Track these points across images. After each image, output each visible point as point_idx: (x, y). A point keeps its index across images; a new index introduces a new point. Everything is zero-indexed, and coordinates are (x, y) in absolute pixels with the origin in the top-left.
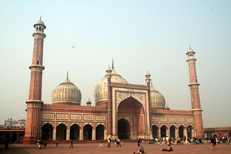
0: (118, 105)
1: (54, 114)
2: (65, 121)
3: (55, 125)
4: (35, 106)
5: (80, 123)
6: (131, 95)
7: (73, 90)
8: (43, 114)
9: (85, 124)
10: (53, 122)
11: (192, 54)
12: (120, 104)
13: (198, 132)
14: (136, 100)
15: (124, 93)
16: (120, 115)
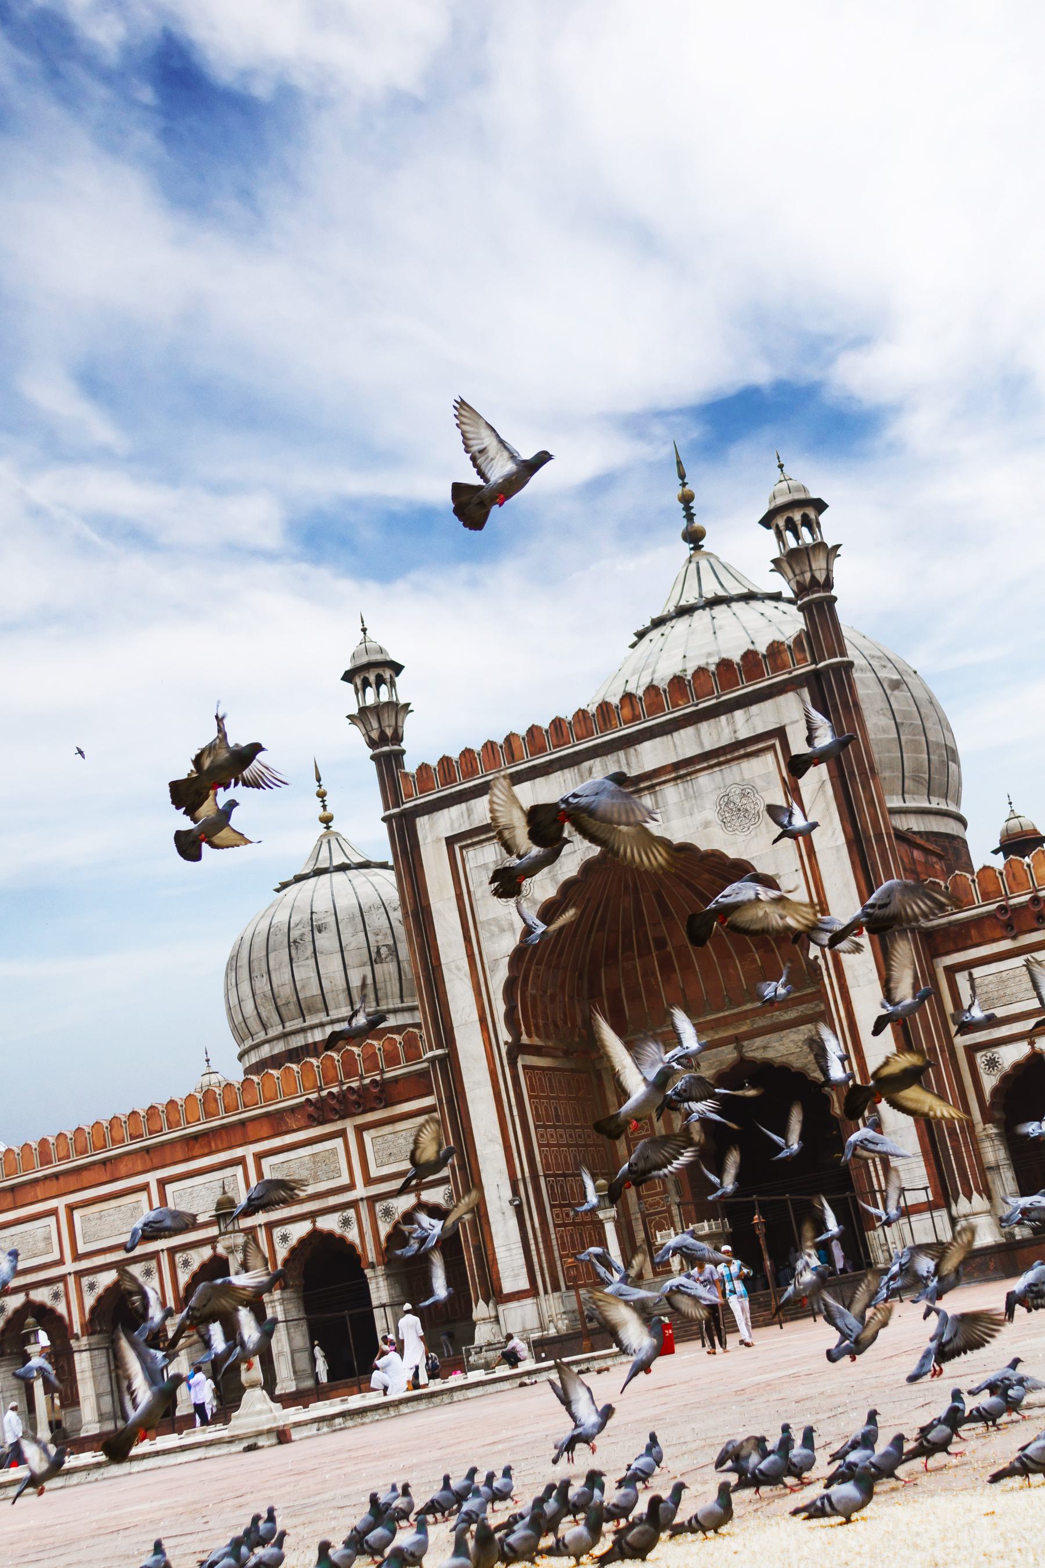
0: (498, 978)
1: (53, 1219)
7: (295, 934)
9: (285, 1238)
10: (61, 1285)
12: (518, 957)
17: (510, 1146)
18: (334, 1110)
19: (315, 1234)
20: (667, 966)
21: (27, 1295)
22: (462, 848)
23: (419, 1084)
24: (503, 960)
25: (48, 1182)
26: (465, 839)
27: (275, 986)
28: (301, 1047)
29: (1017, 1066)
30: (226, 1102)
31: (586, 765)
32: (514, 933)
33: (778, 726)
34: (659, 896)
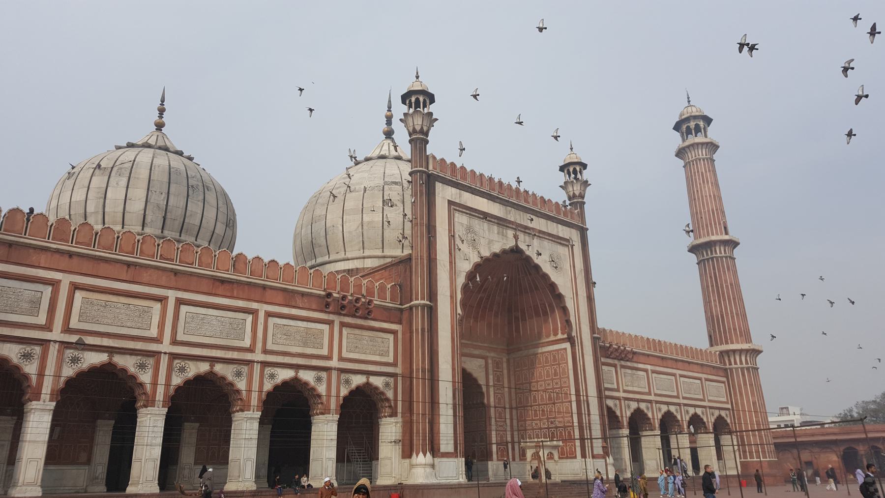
0: (461, 280)
1: (50, 289)
2: (139, 345)
5: (245, 369)
6: (516, 237)
9: (272, 376)
10: (37, 350)
11: (701, 124)
15: (486, 225)
17: (455, 369)
18: (343, 307)
19: (296, 379)
24: (463, 273)
25: (57, 256)
26: (457, 206)
27: (169, 204)
30: (253, 268)
31: (510, 208)
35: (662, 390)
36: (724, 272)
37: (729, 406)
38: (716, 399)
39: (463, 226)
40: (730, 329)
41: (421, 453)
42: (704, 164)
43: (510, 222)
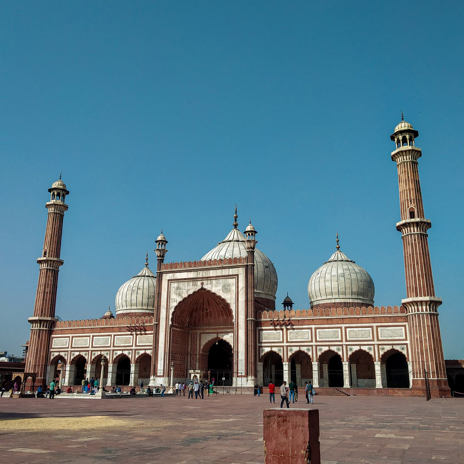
0: (172, 310)
1: (69, 338)
3: (69, 358)
4: (35, 327)
6: (202, 284)
8: (54, 339)
9: (116, 354)
10: (67, 353)
12: (176, 308)
13: (417, 369)
14: (214, 294)
15: (186, 283)
16: (211, 331)
20: (207, 315)
21: (59, 353)
22: (171, 282)
23: (151, 328)
28: (129, 313)
29: (267, 352)
32: (177, 302)
33: (237, 274)
34: (208, 300)
35: (326, 338)
36: (407, 246)
37: (408, 342)
38: (390, 338)
39: (175, 288)
40: (407, 288)
41: (152, 376)
42: (400, 168)
43: (199, 278)
